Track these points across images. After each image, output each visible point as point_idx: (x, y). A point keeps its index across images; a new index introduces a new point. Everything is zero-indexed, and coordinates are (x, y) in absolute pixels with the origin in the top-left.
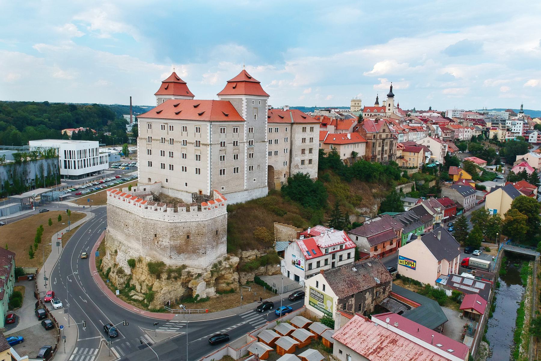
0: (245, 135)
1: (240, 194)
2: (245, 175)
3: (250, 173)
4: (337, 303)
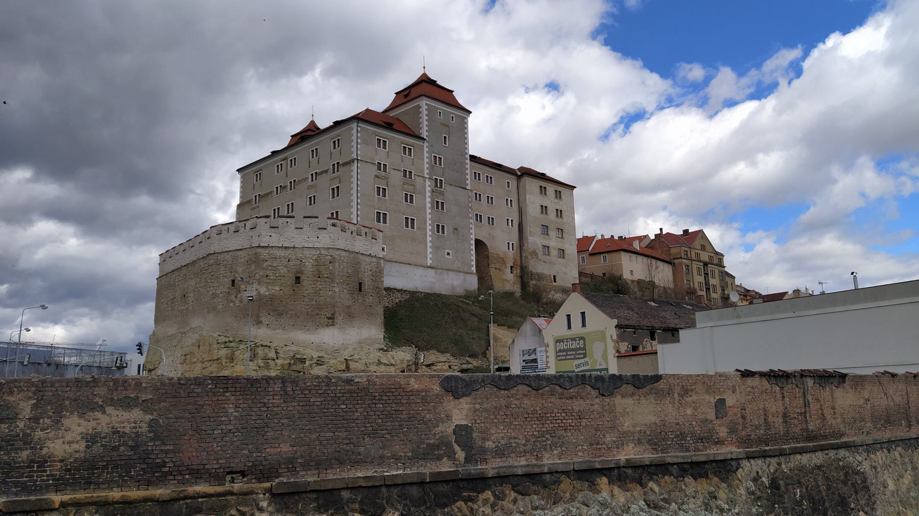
0: (426, 166)
1: (419, 272)
2: (429, 239)
4: (615, 337)
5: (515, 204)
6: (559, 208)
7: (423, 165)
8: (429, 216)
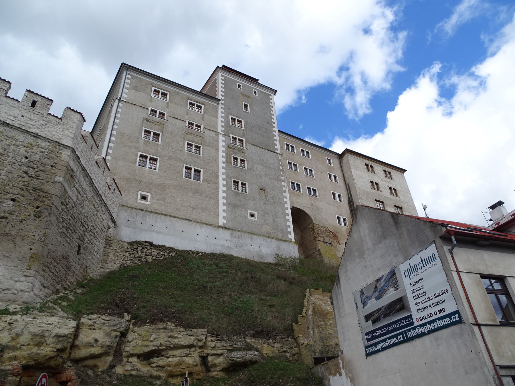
1: (203, 231)
2: (222, 195)
3: (237, 194)
5: (340, 180)
6: (393, 187)
7: (217, 123)
8: (222, 171)
